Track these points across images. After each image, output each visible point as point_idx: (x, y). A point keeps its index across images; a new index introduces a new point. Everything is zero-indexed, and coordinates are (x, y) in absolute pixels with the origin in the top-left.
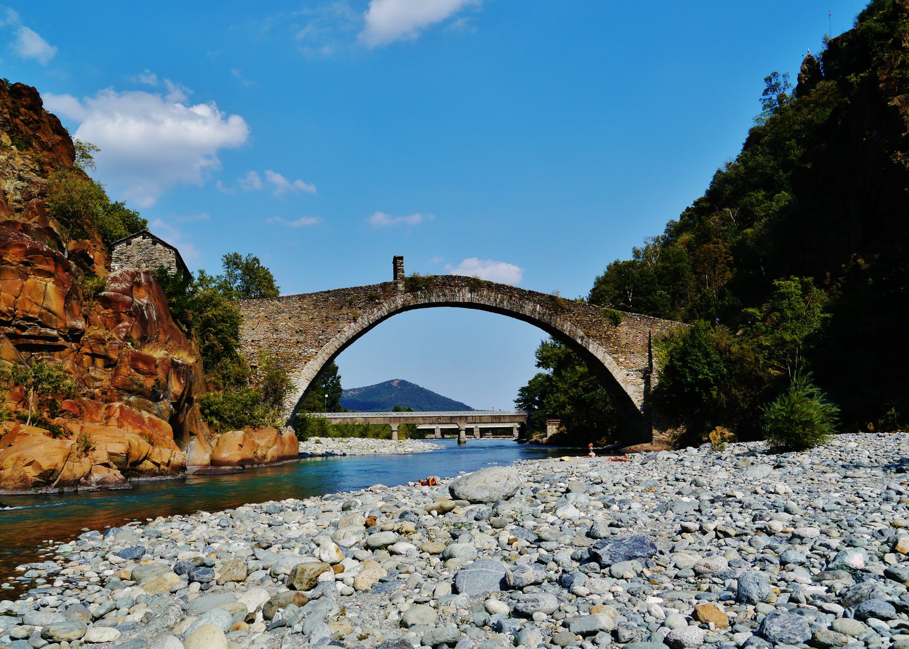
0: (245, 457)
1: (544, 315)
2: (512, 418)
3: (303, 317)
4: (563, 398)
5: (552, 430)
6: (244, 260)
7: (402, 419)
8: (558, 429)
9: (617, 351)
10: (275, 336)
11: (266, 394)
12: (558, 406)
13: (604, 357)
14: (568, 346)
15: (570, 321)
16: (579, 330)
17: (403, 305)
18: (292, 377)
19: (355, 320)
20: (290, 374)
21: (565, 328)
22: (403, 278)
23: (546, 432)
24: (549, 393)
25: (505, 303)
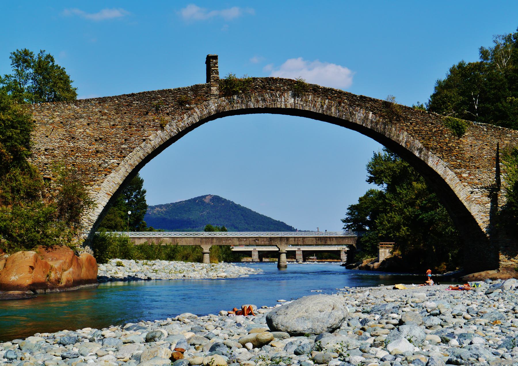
0: (37, 281)
1: (377, 123)
2: (339, 240)
3: (104, 124)
4: (397, 218)
5: (384, 254)
6: (36, 57)
7: (215, 240)
8: (391, 253)
9: (460, 165)
10: (72, 145)
11: (61, 210)
12: (392, 227)
13: (445, 172)
14: (404, 159)
15: (407, 130)
16: (417, 141)
17: (216, 111)
18: (90, 192)
19: (162, 127)
20: (89, 187)
21: (401, 138)
22: (217, 80)
23: (378, 256)
24: (382, 212)
25: (333, 109)
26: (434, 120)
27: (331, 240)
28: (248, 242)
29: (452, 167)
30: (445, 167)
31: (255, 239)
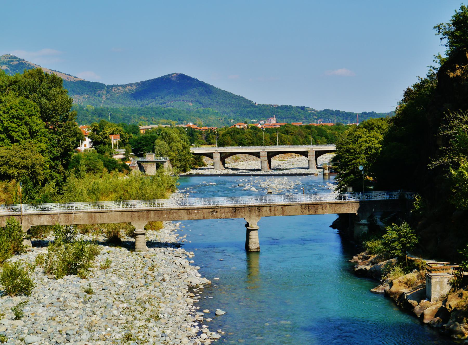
27: (324, 207)
28: (202, 216)
31: (211, 210)
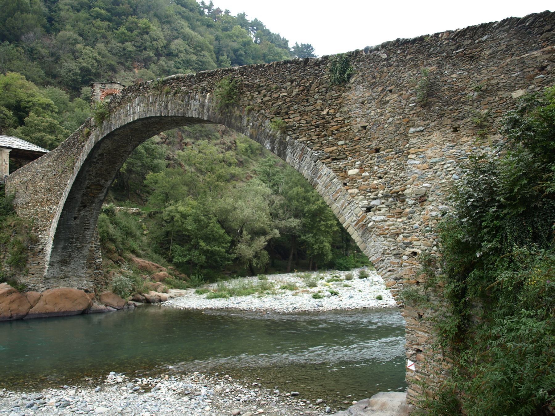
13: (315, 172)
20: (45, 232)
26: (295, 72)
29: (327, 158)
30: (315, 162)
